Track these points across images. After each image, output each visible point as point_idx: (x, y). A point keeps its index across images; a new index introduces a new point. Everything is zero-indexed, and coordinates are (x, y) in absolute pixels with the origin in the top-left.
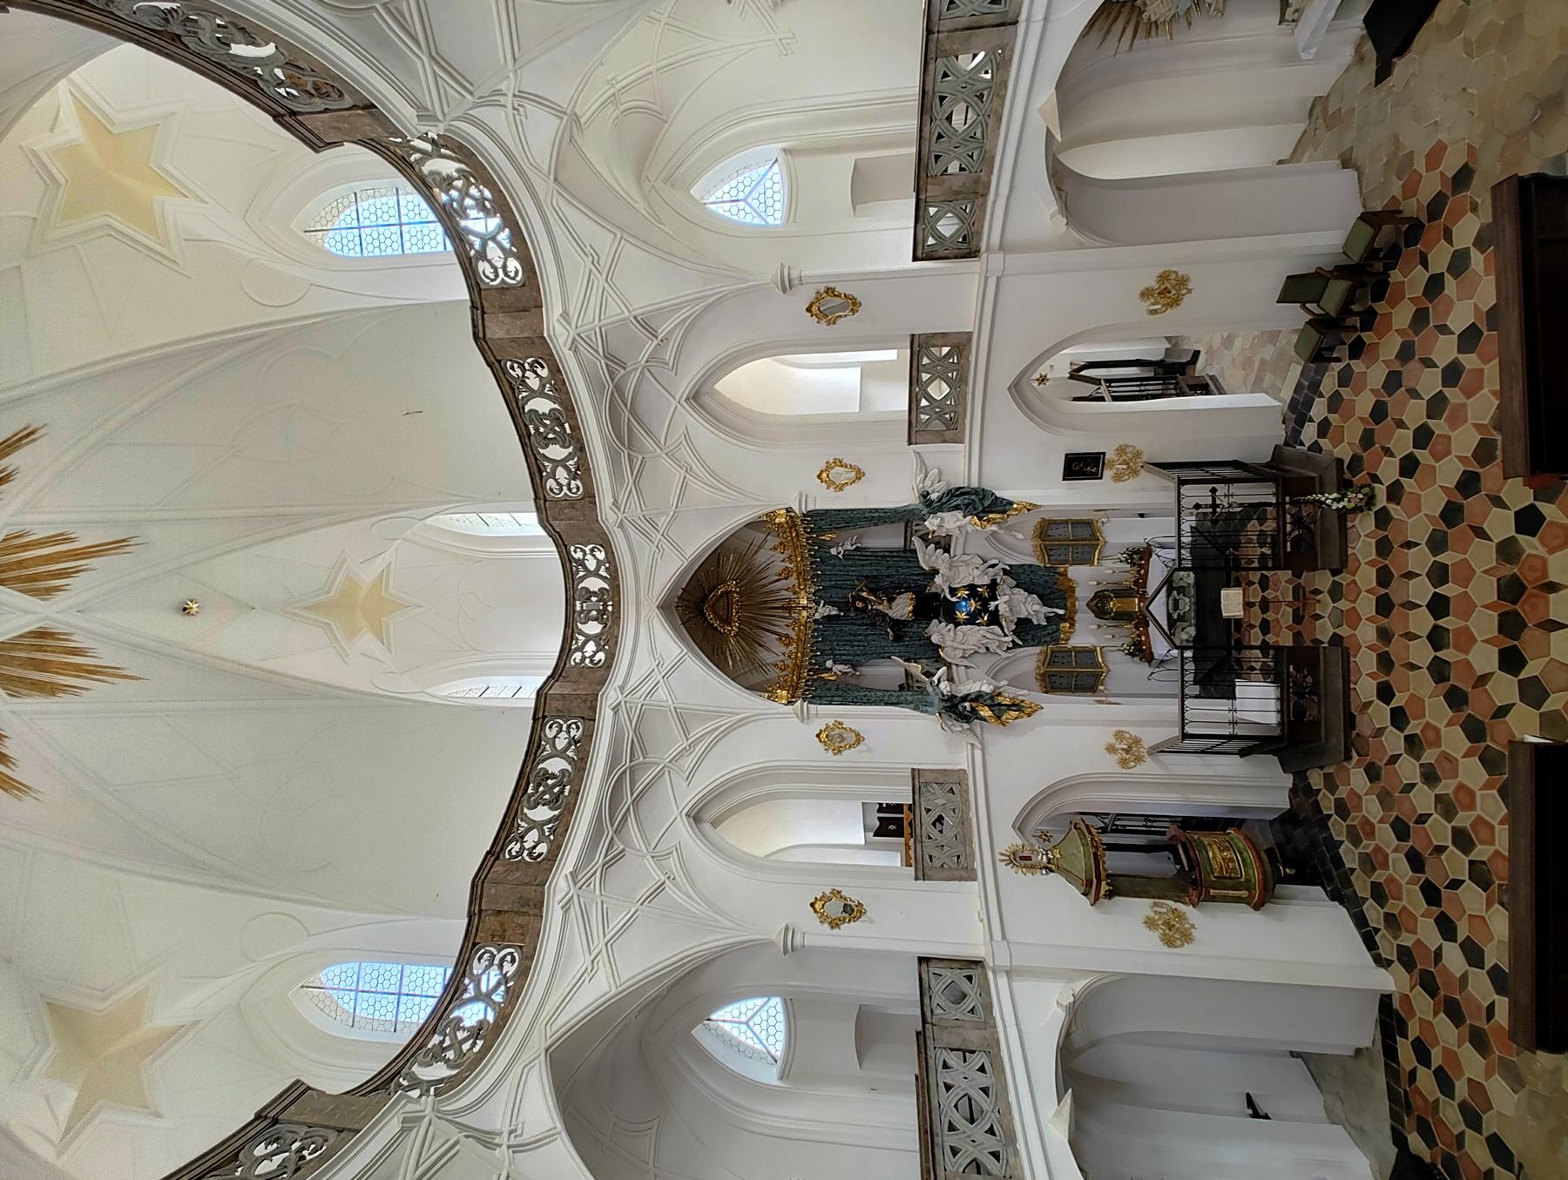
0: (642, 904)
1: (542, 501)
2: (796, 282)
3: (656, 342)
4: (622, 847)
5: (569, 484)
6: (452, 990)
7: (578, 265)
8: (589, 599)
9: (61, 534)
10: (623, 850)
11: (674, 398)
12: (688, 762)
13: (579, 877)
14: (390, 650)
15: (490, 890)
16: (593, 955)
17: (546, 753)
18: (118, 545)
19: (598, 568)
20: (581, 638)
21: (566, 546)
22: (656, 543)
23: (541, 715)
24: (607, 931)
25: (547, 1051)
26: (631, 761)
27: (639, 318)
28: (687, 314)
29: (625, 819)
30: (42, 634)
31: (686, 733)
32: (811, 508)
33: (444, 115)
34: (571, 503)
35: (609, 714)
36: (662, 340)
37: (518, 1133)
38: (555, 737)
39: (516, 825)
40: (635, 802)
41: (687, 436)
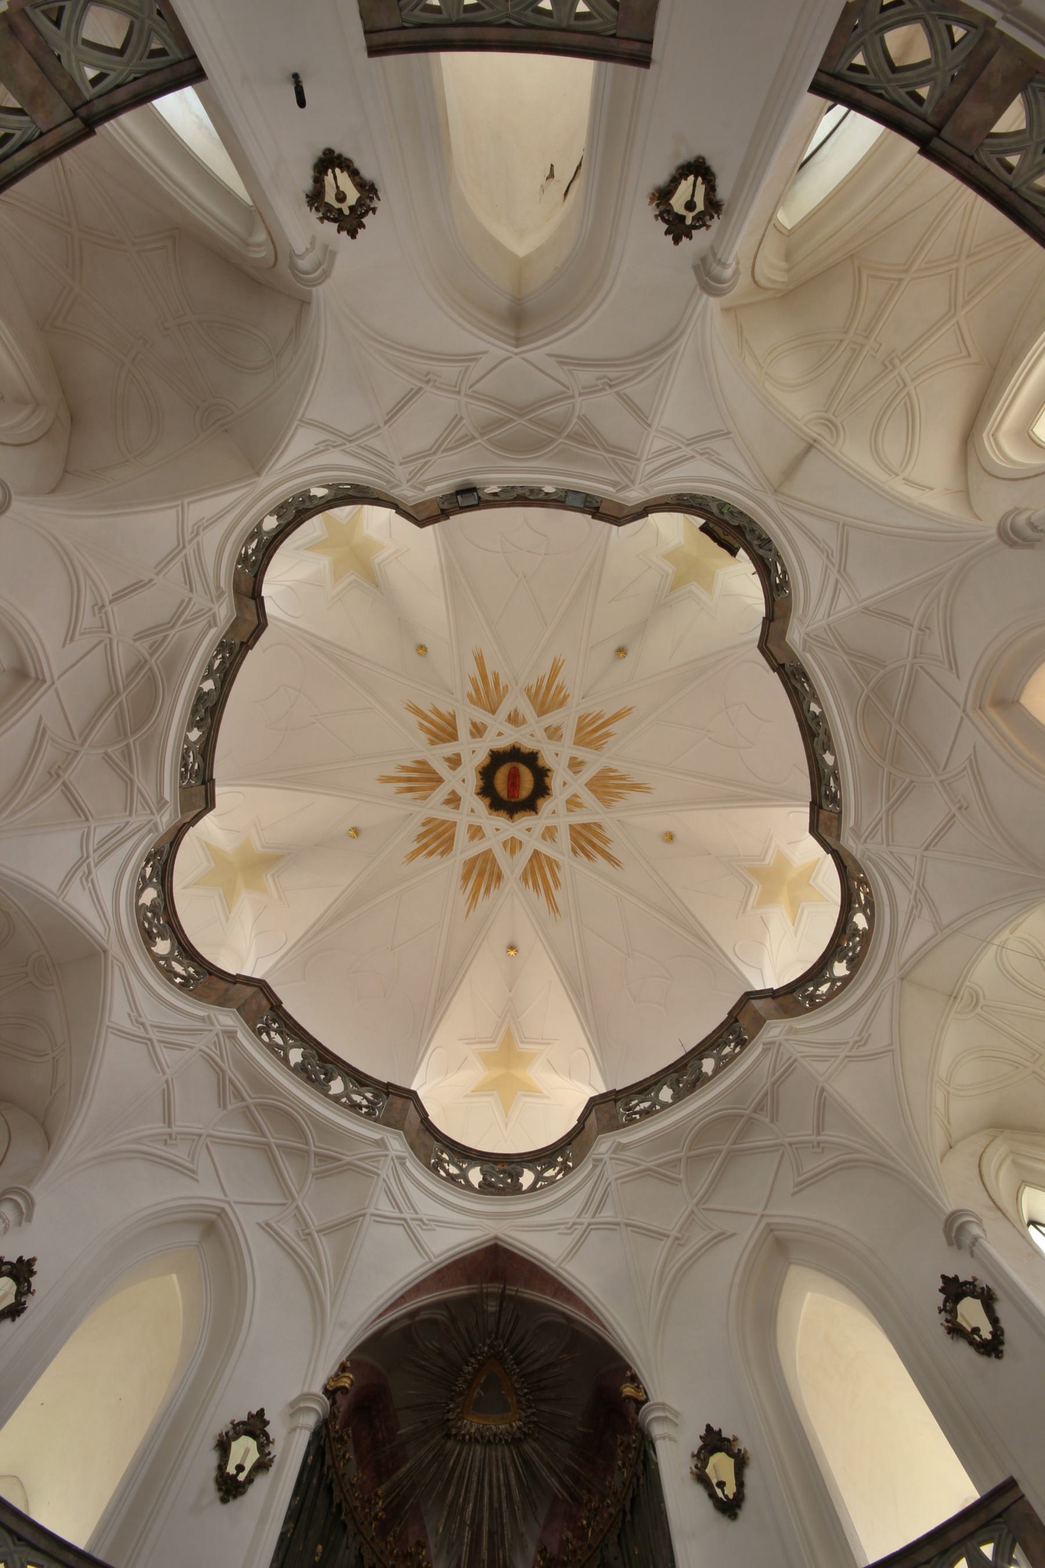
0: (167, 1082)
1: (614, 1097)
2: (967, 1241)
3: (813, 1138)
4: (229, 1107)
5: (636, 1113)
6: (187, 948)
7: (847, 1031)
8: (511, 1176)
9: (559, 883)
10: (225, 1107)
11: (765, 1208)
12: (288, 1230)
13: (227, 1041)
14: (467, 1096)
15: (249, 990)
16: (148, 1027)
17: (351, 1086)
18: (554, 908)
19: (546, 1179)
20: (464, 1166)
21: (569, 1144)
22: (578, 1220)
23: (390, 1090)
24: (162, 1045)
25: (105, 951)
26: (316, 1154)
27: (825, 1094)
28: (857, 1146)
29: (255, 1127)
30: (499, 876)
31: (328, 1230)
32: (657, 1430)
33: (865, 842)
34: (614, 1117)
35: (377, 1136)
36: (819, 1143)
37: (84, 879)
38: (365, 1098)
39: (293, 1036)
40: (266, 1149)
41: (722, 1237)
